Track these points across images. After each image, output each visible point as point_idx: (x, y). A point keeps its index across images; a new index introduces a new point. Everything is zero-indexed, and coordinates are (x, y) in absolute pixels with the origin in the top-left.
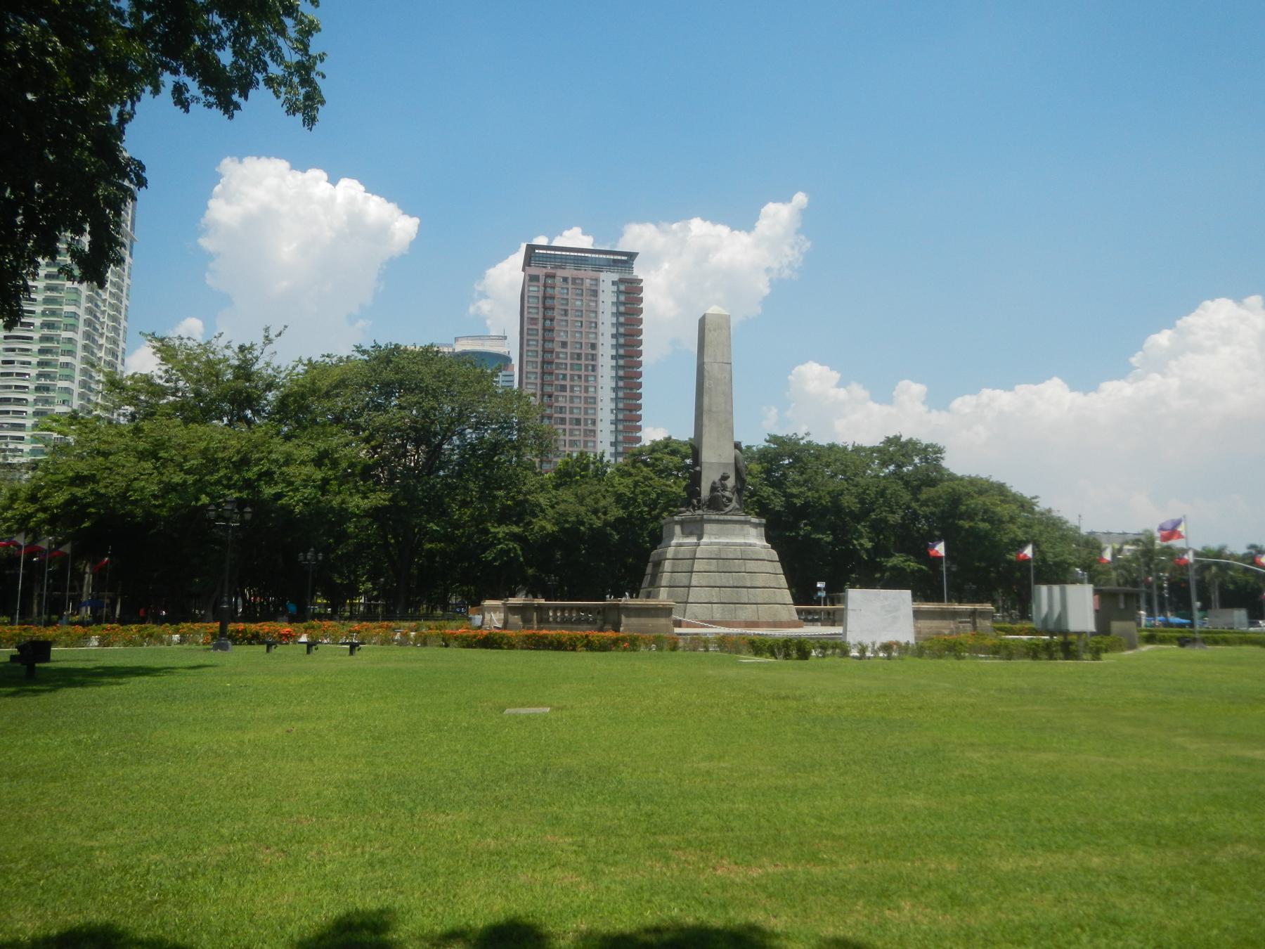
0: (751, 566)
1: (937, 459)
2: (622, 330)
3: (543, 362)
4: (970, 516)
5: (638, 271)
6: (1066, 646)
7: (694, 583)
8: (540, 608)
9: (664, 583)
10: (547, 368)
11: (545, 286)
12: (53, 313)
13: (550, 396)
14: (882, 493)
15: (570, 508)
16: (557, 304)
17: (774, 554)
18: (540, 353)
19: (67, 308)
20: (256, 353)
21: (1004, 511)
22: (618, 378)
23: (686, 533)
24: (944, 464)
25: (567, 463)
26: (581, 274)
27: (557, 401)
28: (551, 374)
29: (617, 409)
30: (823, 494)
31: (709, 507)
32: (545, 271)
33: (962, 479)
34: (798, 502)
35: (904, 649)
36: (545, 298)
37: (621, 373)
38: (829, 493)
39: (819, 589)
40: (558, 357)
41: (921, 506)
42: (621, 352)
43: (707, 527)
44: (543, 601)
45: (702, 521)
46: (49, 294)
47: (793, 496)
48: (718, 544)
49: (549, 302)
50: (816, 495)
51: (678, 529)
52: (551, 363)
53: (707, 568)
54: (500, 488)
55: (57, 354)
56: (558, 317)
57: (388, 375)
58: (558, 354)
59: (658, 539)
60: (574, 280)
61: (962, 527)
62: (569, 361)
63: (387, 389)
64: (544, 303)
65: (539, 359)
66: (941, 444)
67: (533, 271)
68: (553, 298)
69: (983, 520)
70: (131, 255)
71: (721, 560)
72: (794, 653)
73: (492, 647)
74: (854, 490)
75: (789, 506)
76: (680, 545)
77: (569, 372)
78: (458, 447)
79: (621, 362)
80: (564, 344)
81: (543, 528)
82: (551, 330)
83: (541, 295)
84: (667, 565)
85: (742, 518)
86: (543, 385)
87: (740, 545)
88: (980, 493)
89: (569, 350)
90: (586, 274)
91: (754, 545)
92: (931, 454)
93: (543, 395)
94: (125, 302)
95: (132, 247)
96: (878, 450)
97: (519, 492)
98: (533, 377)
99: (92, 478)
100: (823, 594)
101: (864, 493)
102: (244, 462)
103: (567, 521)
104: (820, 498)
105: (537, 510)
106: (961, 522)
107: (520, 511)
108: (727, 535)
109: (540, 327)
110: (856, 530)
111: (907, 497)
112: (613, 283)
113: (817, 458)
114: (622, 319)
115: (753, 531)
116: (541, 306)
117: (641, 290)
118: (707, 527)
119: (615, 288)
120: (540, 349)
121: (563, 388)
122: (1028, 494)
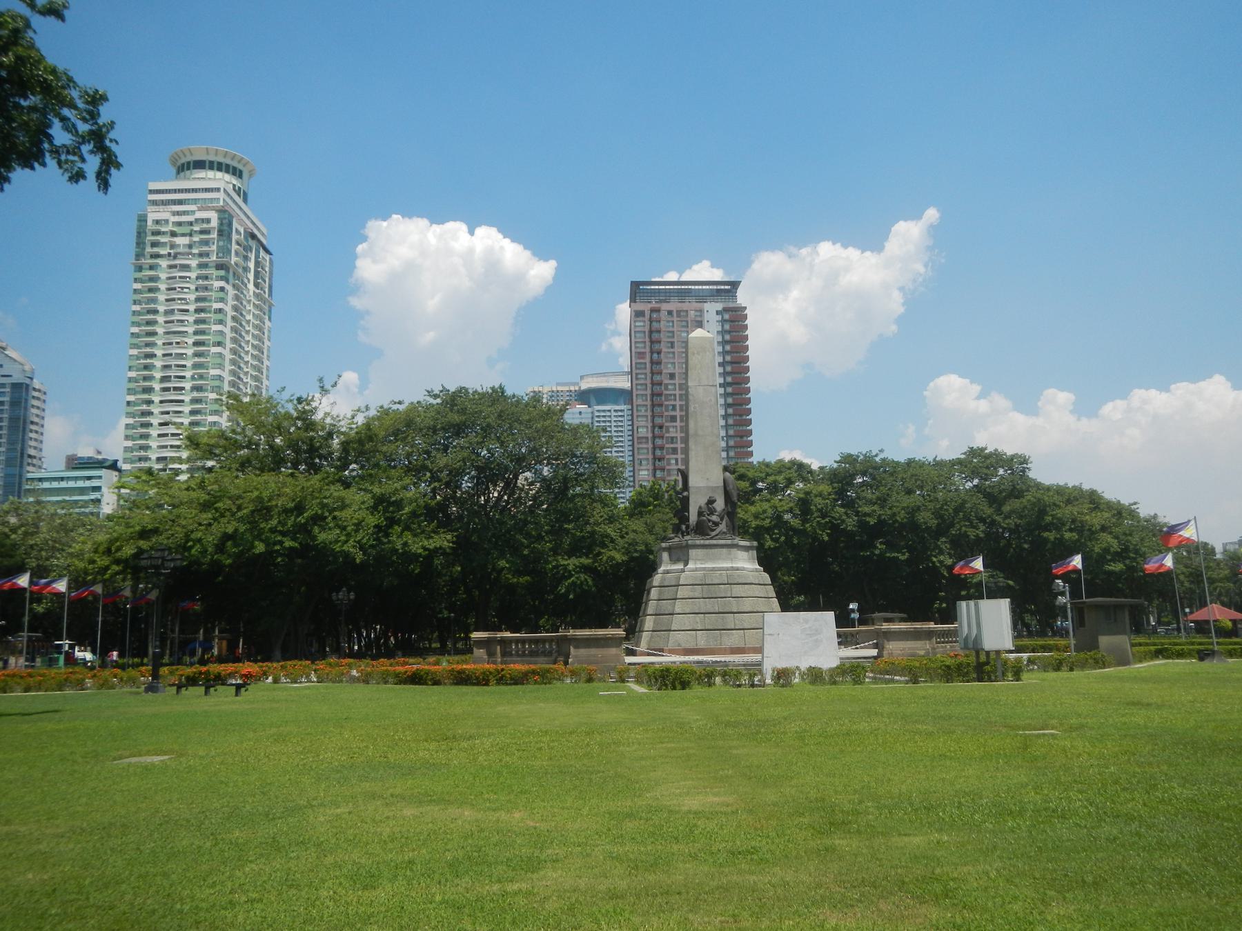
0: (738, 590)
1: (1023, 471)
2: (728, 358)
3: (653, 395)
4: (1058, 525)
5: (742, 297)
6: (983, 667)
7: (677, 610)
8: (503, 642)
9: (650, 611)
10: (657, 400)
12: (201, 377)
13: (661, 427)
14: (957, 510)
15: (639, 538)
16: (664, 337)
17: (766, 578)
18: (649, 386)
19: (213, 372)
20: (314, 404)
21: (1095, 520)
22: (727, 406)
23: (674, 560)
24: (1031, 475)
25: (640, 494)
26: (685, 306)
27: (668, 431)
28: (661, 405)
29: (727, 436)
31: (696, 533)
32: (650, 306)
33: (1048, 489)
34: (872, 521)
35: (815, 675)
36: (651, 332)
37: (730, 400)
38: (903, 508)
39: (853, 610)
40: (666, 389)
41: (1006, 517)
42: (729, 379)
43: (693, 552)
44: (508, 634)
45: (688, 547)
46: (197, 359)
47: (866, 515)
48: (704, 569)
49: (655, 336)
50: (889, 512)
51: (665, 555)
52: (660, 395)
53: (691, 594)
54: (570, 522)
55: (205, 414)
56: (664, 350)
57: (457, 418)
58: (667, 385)
59: (652, 568)
60: (679, 312)
61: (1046, 540)
62: (677, 392)
63: (458, 430)
64: (650, 337)
65: (649, 392)
66: (1027, 455)
67: (639, 306)
68: (659, 332)
69: (1071, 530)
70: (270, 319)
71: (707, 586)
72: (679, 686)
73: (416, 684)
74: (931, 506)
75: (862, 525)
76: (668, 572)
77: (678, 403)
78: (544, 480)
79: (729, 390)
80: (672, 376)
81: (612, 558)
82: (659, 363)
83: (647, 329)
84: (654, 593)
85: (729, 542)
86: (653, 417)
87: (727, 569)
88: (1069, 502)
89: (677, 381)
90: (690, 306)
91: (743, 569)
92: (1017, 465)
93: (653, 427)
94: (266, 362)
96: (959, 462)
97: (587, 523)
98: (643, 409)
99: (156, 531)
100: (856, 616)
101: (941, 508)
102: (299, 508)
103: (636, 551)
104: (894, 514)
105: (607, 541)
106: (1046, 534)
107: (588, 544)
109: (648, 360)
110: (937, 547)
111: (988, 511)
112: (718, 313)
113: (892, 474)
114: (728, 348)
115: (742, 555)
116: (647, 339)
117: (745, 317)
118: (693, 552)
119: (719, 318)
120: (649, 381)
121: (673, 419)
122: (1125, 501)
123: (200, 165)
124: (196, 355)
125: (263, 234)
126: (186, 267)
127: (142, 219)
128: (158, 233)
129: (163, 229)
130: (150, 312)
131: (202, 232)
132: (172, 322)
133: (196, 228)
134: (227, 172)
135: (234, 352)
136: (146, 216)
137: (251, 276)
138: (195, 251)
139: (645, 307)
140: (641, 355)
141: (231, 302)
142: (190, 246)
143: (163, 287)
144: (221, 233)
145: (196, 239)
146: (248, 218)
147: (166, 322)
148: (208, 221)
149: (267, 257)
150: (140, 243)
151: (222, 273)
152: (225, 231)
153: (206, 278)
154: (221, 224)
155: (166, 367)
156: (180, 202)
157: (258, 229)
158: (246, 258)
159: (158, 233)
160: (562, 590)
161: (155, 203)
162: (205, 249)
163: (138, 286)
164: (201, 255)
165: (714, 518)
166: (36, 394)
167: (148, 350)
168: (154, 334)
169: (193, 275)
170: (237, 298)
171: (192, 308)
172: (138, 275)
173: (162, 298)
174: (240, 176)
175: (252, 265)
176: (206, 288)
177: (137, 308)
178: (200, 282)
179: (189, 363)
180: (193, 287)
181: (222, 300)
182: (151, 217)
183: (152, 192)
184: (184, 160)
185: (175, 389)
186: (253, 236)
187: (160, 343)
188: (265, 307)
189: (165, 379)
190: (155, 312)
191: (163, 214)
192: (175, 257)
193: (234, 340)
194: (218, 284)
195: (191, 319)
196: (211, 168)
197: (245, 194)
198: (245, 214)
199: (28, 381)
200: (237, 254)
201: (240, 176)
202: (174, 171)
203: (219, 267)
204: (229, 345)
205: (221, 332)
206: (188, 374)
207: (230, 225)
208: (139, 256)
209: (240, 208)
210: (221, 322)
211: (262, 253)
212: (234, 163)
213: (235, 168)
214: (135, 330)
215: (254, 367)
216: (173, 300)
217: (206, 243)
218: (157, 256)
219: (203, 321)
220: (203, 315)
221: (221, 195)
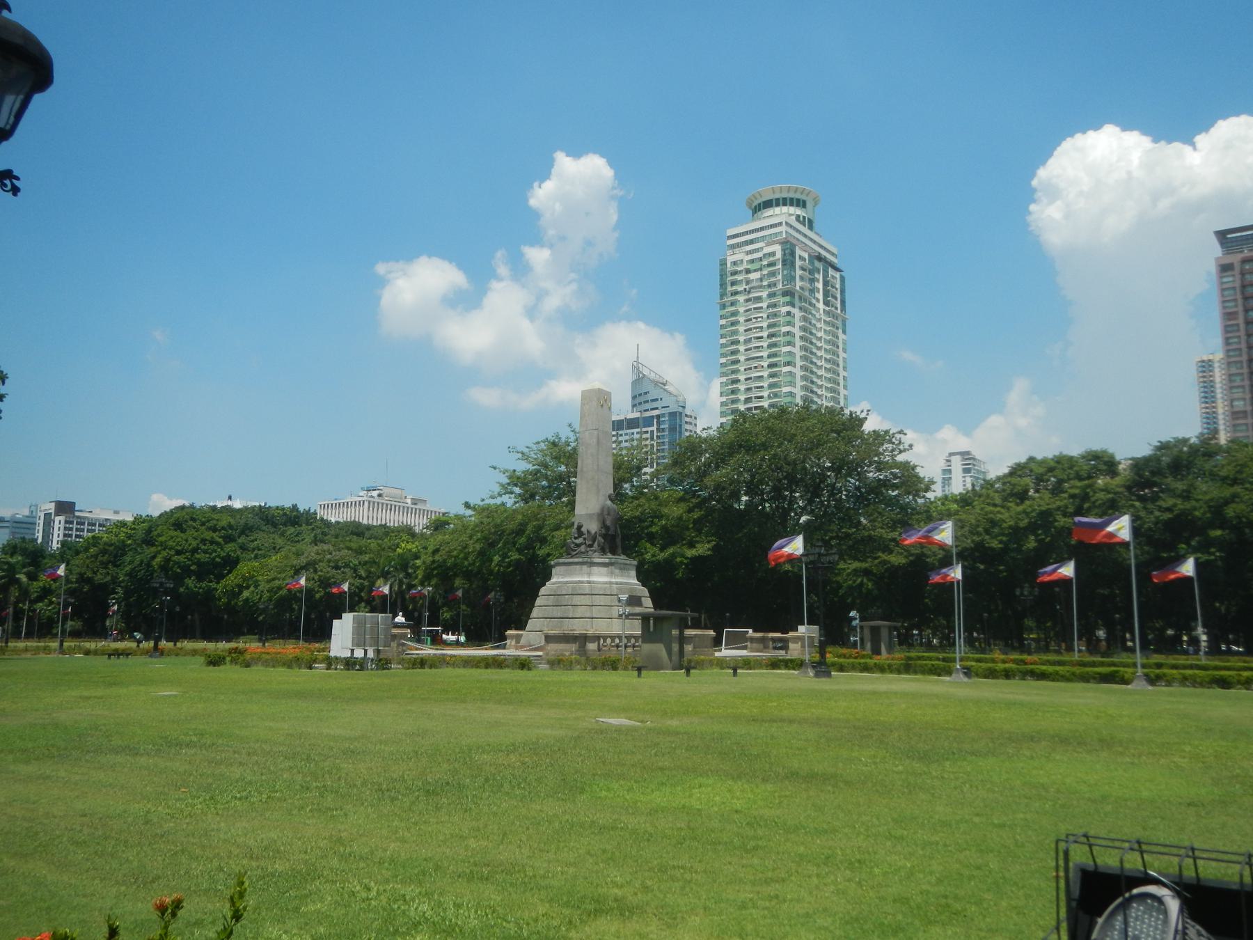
11: (1243, 274)
19: (786, 390)
30: (1197, 505)
32: (1239, 257)
36: (1244, 287)
38: (1206, 502)
64: (1243, 293)
65: (1245, 358)
70: (844, 332)
83: (1238, 284)
94: (842, 374)
95: (844, 325)
98: (1238, 379)
108: (571, 574)
109: (1241, 321)
116: (1239, 296)
123: (768, 204)
124: (772, 376)
125: (833, 254)
126: (759, 299)
127: (723, 263)
130: (733, 343)
131: (770, 265)
133: (765, 263)
134: (791, 205)
135: (804, 368)
137: (820, 296)
138: (765, 283)
139: (1236, 259)
140: (1229, 316)
141: (798, 323)
142: (761, 280)
143: (742, 319)
144: (784, 262)
145: (765, 272)
146: (815, 242)
148: (774, 254)
149: (838, 275)
150: (723, 285)
151: (788, 299)
152: (789, 259)
153: (775, 305)
154: (784, 255)
155: (749, 389)
156: (751, 242)
157: (828, 251)
158: (812, 281)
160: (841, 592)
161: (733, 247)
162: (772, 279)
163: (723, 322)
164: (769, 286)
165: (579, 541)
166: (688, 420)
168: (737, 362)
169: (764, 305)
170: (804, 319)
171: (765, 334)
172: (723, 312)
173: (741, 329)
174: (804, 206)
175: (820, 286)
176: (775, 315)
177: (723, 341)
178: (771, 310)
179: (765, 384)
180: (765, 316)
181: (789, 323)
182: (730, 259)
183: (730, 238)
184: (756, 203)
186: (820, 258)
187: (742, 369)
188: (838, 321)
190: (737, 342)
191: (739, 255)
193: (804, 358)
194: (784, 309)
195: (765, 344)
196: (777, 205)
197: (810, 222)
198: (811, 240)
199: (680, 410)
200: (802, 278)
201: (804, 206)
203: (785, 294)
204: (799, 363)
205: (790, 353)
206: (765, 394)
207: (793, 254)
208: (722, 296)
209: (805, 236)
210: (789, 343)
211: (831, 272)
212: (798, 196)
213: (798, 200)
214: (723, 360)
215: (829, 380)
217: (773, 274)
218: (735, 293)
220: (774, 339)
221: (783, 228)
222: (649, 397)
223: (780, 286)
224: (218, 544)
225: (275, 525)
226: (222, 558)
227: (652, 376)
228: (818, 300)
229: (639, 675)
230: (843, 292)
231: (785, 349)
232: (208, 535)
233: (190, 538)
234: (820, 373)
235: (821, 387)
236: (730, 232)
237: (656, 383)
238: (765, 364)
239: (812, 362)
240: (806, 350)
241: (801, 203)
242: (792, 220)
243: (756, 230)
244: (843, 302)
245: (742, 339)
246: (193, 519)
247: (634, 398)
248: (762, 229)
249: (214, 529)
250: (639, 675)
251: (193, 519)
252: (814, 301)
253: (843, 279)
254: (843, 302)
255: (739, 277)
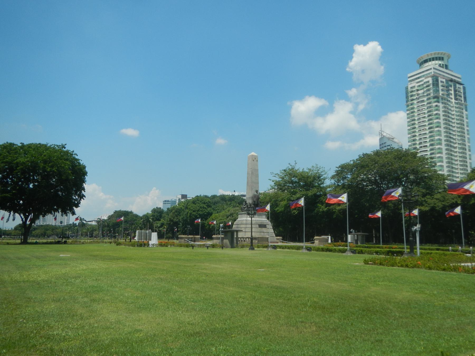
12: (432, 140)
19: (436, 138)
46: (430, 134)
55: (435, 154)
105: (424, 203)
123: (426, 61)
124: (430, 132)
125: (459, 78)
126: (423, 101)
127: (407, 88)
128: (412, 92)
129: (414, 90)
132: (420, 122)
133: (425, 86)
136: (408, 87)
138: (425, 94)
142: (424, 93)
143: (416, 110)
145: (425, 90)
146: (449, 74)
147: (419, 123)
148: (428, 82)
149: (461, 87)
150: (407, 97)
151: (436, 100)
153: (430, 103)
154: (433, 81)
156: (419, 78)
158: (448, 90)
159: (412, 92)
162: (428, 92)
164: (427, 95)
167: (414, 134)
168: (415, 128)
169: (425, 103)
171: (426, 115)
173: (416, 114)
175: (452, 92)
176: (430, 107)
178: (428, 105)
179: (428, 136)
180: (426, 108)
182: (410, 86)
183: (409, 77)
184: (421, 61)
185: (424, 146)
186: (451, 80)
187: (417, 131)
188: (463, 106)
189: (420, 143)
190: (414, 120)
191: (414, 84)
192: (418, 99)
194: (434, 104)
195: (426, 120)
196: (430, 61)
200: (442, 90)
202: (418, 65)
203: (434, 98)
206: (428, 140)
207: (437, 80)
208: (407, 101)
209: (444, 72)
211: (458, 86)
212: (439, 56)
216: (419, 114)
217: (429, 90)
219: (431, 120)
220: (430, 117)
221: (432, 71)
222: (387, 144)
223: (432, 95)
224: (205, 208)
225: (226, 201)
226: (207, 213)
227: (388, 136)
228: (452, 99)
229: (193, 248)
230: (465, 93)
231: (435, 121)
232: (202, 205)
233: (196, 207)
234: (454, 129)
235: (455, 135)
236: (409, 75)
237: (389, 139)
238: (427, 128)
239: (449, 125)
240: (446, 120)
241: (441, 59)
242: (437, 67)
243: (421, 73)
244: (465, 98)
245: (416, 118)
246: (198, 200)
247: (380, 145)
248: (423, 72)
249: (204, 203)
250: (193, 248)
251: (198, 200)
252: (449, 99)
253: (464, 88)
254: (465, 98)
255: (414, 93)
